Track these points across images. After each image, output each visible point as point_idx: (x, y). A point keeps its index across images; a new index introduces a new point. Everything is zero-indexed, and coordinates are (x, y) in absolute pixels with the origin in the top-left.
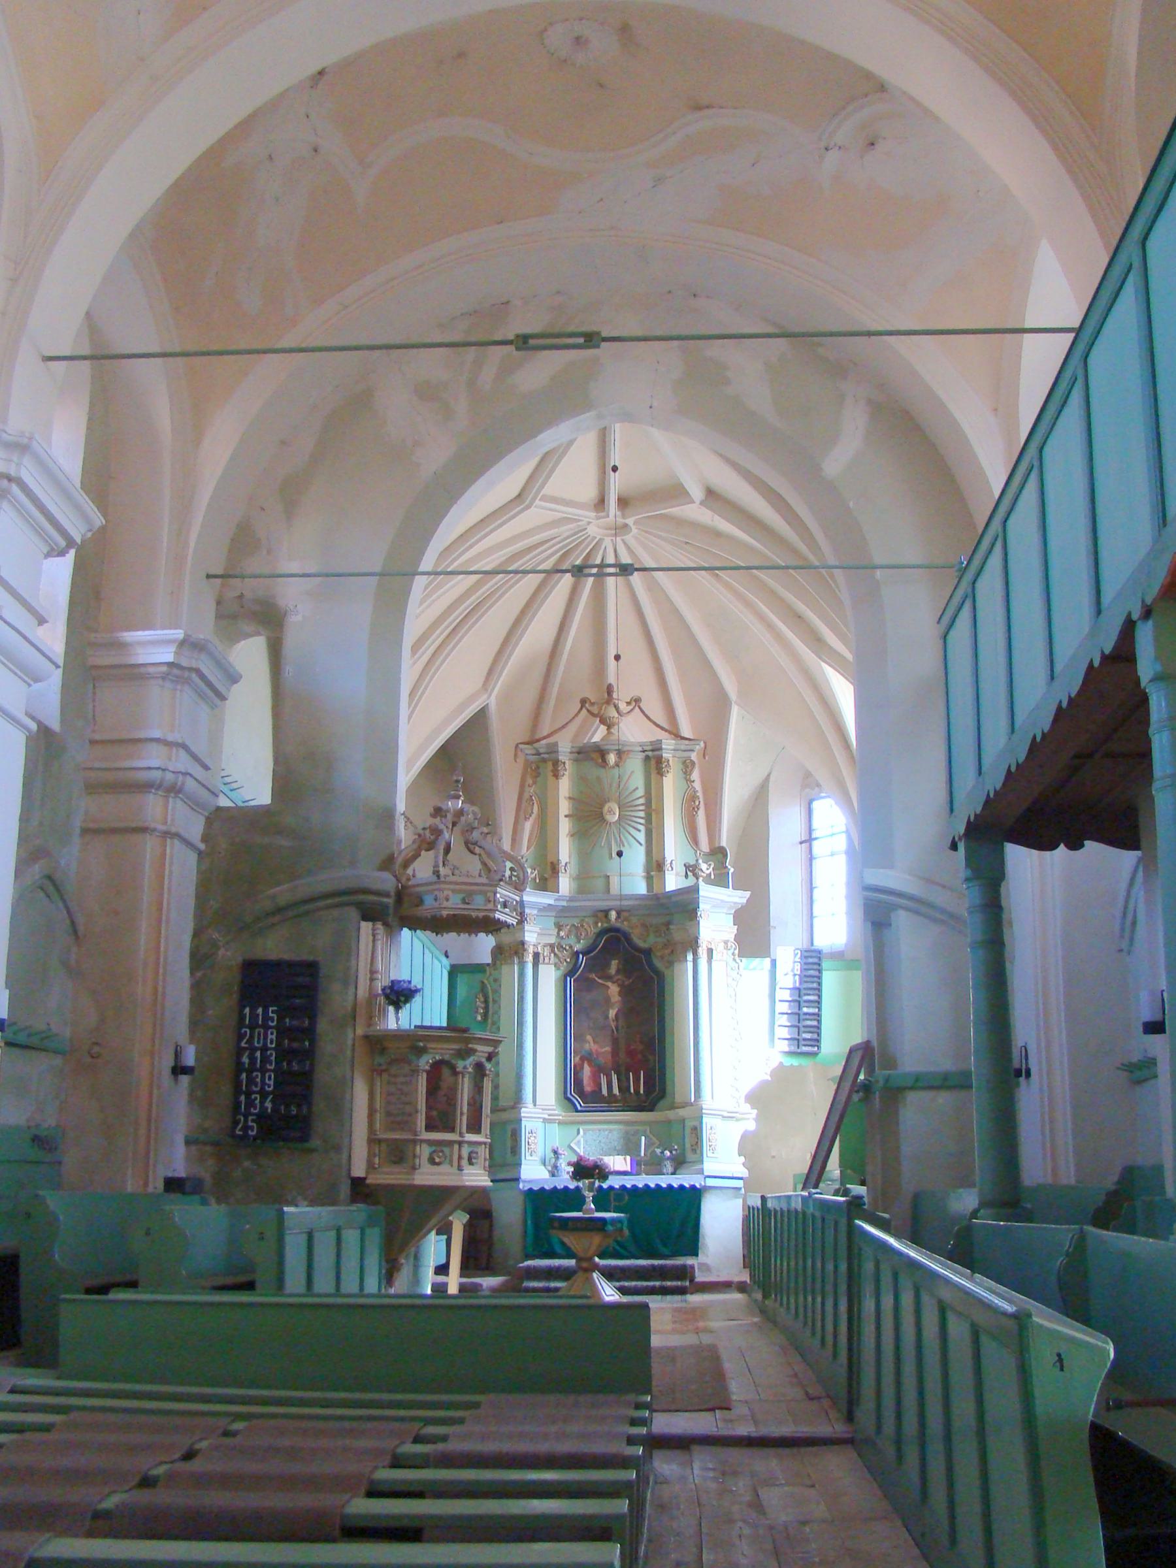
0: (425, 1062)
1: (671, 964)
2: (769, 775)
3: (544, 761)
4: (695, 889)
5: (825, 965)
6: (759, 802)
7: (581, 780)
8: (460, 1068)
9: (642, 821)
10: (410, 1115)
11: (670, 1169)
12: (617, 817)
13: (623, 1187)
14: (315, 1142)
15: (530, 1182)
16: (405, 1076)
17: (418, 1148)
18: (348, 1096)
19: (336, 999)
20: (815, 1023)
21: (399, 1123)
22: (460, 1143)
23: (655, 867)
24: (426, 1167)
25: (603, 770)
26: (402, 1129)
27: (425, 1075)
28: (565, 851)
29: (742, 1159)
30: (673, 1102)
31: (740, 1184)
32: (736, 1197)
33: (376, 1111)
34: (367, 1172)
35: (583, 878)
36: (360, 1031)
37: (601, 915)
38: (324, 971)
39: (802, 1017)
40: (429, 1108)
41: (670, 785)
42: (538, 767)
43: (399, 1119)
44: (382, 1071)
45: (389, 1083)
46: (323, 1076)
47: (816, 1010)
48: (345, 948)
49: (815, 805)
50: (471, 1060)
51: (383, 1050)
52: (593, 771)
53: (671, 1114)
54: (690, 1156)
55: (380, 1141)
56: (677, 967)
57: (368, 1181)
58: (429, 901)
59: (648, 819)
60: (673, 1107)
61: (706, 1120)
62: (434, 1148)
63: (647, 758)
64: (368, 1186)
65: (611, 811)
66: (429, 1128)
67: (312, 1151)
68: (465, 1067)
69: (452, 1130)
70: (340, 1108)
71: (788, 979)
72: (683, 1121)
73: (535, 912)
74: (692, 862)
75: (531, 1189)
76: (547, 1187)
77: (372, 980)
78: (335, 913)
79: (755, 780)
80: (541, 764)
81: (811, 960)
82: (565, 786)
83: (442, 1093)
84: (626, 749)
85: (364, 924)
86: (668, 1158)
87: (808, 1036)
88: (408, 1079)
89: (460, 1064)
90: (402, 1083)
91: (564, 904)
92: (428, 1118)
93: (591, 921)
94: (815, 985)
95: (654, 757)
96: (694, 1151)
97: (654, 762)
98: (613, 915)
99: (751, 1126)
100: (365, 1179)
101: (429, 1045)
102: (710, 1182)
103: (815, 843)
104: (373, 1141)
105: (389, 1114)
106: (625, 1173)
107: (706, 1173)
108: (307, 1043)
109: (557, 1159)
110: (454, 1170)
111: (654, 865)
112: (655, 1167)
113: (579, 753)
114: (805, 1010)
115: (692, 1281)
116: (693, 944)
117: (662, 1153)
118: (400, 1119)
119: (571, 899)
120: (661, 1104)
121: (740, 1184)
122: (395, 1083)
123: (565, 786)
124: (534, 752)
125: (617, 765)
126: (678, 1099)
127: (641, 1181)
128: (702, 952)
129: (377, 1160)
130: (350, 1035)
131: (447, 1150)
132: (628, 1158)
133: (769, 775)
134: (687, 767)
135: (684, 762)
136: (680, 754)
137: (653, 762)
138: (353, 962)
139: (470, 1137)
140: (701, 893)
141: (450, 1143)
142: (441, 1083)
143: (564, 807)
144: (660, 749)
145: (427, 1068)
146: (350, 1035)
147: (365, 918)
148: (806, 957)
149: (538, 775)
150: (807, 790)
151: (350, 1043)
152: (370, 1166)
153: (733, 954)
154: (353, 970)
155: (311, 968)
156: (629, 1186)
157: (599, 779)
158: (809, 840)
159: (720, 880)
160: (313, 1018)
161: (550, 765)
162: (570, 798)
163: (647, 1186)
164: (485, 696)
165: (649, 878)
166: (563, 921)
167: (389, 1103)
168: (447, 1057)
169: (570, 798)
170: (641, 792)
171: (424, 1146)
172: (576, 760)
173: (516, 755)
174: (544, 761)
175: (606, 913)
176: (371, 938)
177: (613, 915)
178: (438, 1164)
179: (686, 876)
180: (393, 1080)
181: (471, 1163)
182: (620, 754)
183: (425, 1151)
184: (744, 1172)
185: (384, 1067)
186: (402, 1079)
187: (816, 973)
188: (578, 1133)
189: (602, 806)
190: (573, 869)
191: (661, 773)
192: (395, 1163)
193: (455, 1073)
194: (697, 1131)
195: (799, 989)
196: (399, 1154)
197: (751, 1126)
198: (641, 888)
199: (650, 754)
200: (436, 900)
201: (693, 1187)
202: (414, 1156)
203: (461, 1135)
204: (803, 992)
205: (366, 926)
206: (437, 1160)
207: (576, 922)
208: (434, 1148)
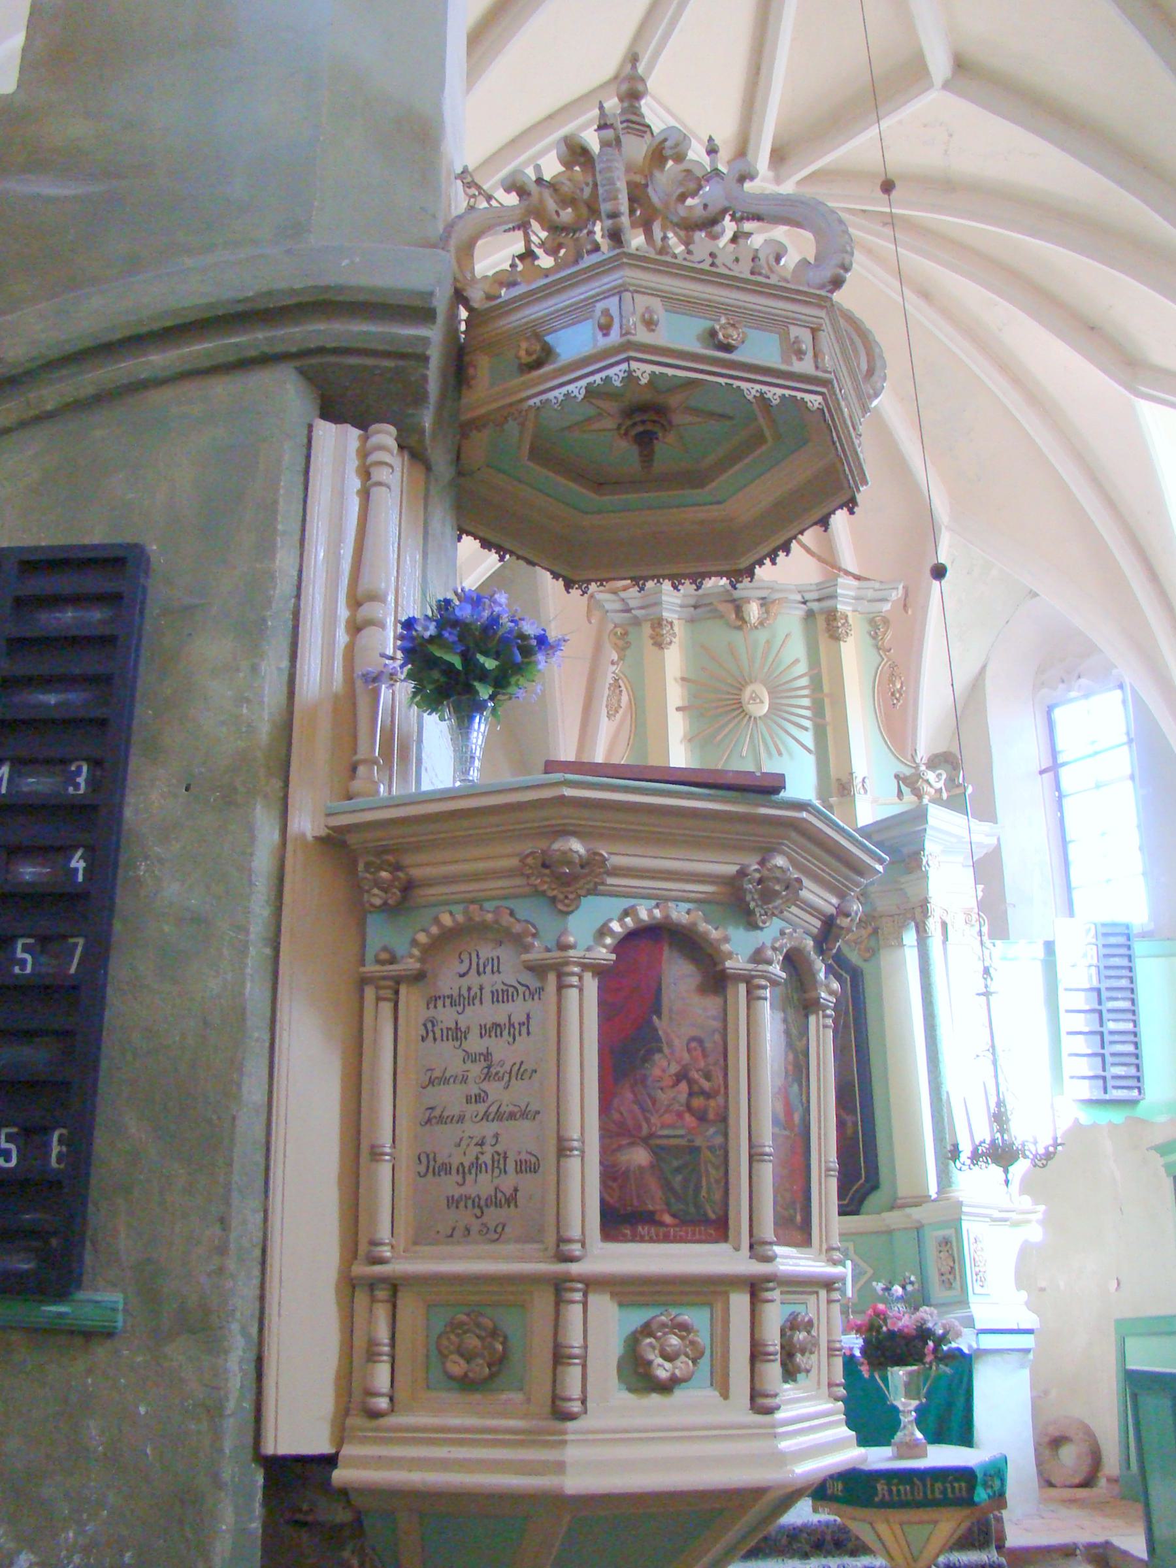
0: (592, 928)
1: (872, 953)
2: (984, 668)
3: (637, 622)
4: (919, 816)
5: (1139, 947)
6: (969, 708)
7: (699, 651)
8: (737, 962)
9: (808, 713)
10: (529, 1166)
14: (103, 1297)
16: (502, 996)
17: (574, 1313)
18: (253, 1090)
19: (208, 694)
20: (1130, 1048)
21: (479, 1205)
22: (559, 1286)
24: (609, 1403)
25: (737, 636)
26: (496, 1234)
27: (591, 985)
29: (1023, 1295)
30: (895, 1199)
31: (1027, 1341)
32: (1022, 1366)
33: (376, 1155)
34: (341, 1435)
36: (306, 823)
38: (163, 590)
39: (1107, 1038)
40: (615, 1132)
41: (854, 658)
42: (626, 634)
43: (483, 1186)
44: (398, 980)
45: (429, 1029)
46: (141, 1006)
47: (1129, 1026)
48: (250, 508)
49: (1057, 714)
50: (773, 933)
51: (404, 898)
52: (718, 635)
53: (893, 1219)
55: (395, 1286)
56: (886, 958)
57: (340, 1475)
58: (574, 342)
59: (818, 709)
60: (894, 1205)
61: (970, 1228)
62: (637, 1317)
63: (810, 615)
64: (344, 1493)
65: (755, 698)
66: (621, 1219)
67: (89, 1335)
68: (758, 957)
69: (717, 1228)
70: (215, 1140)
71: (1079, 970)
72: (919, 1228)
74: (907, 771)
77: (356, 628)
78: (221, 388)
79: (963, 678)
81: (1112, 940)
82: (674, 660)
83: (662, 1067)
84: (777, 596)
85: (326, 431)
86: (900, 1299)
87: (1120, 1071)
88: (517, 1009)
89: (738, 946)
90: (492, 1030)
92: (611, 1175)
94: (1124, 983)
95: (822, 611)
96: (949, 1285)
99: (1035, 1233)
100: (330, 1461)
101: (618, 856)
102: (987, 1342)
103: (1063, 772)
104: (365, 1284)
105: (431, 1166)
107: (979, 1326)
108: (78, 863)
110: (738, 1410)
111: (834, 786)
113: (695, 607)
114: (1112, 1026)
115: (1000, 1548)
116: (916, 913)
117: (887, 1289)
118: (482, 1191)
120: (874, 1200)
121: (1027, 1341)
122: (458, 1034)
123: (674, 660)
124: (618, 606)
125: (761, 623)
126: (904, 1190)
128: (933, 925)
129: (381, 1376)
130: (267, 834)
131: (698, 1318)
133: (984, 668)
134: (877, 626)
135: (872, 622)
136: (864, 606)
137: (821, 622)
138: (284, 560)
139: (791, 1260)
140: (931, 820)
141: (709, 1290)
142: (661, 1025)
143: (675, 695)
144: (833, 596)
145: (603, 954)
146: (267, 834)
147: (331, 411)
148: (1105, 935)
149: (628, 644)
150: (1044, 691)
151: (263, 861)
152: (355, 1406)
153: (980, 933)
154: (284, 587)
155: (108, 575)
157: (732, 650)
158: (1053, 768)
159: (955, 801)
160: (111, 774)
161: (647, 629)
162: (683, 679)
167: (433, 1118)
168: (679, 914)
169: (683, 679)
170: (802, 668)
171: (601, 1303)
172: (691, 621)
174: (637, 622)
176: (355, 483)
178: (666, 1387)
179: (900, 794)
180: (446, 1016)
181: (790, 1373)
182: (764, 603)
183: (602, 1329)
184: (1029, 1320)
185: (411, 965)
186: (490, 1013)
187: (1124, 962)
189: (740, 690)
191: (835, 636)
192: (466, 1384)
193: (716, 980)
194: (951, 1247)
195: (1099, 991)
196: (484, 1347)
197: (1035, 1233)
199: (815, 606)
200: (605, 329)
202: (559, 1357)
203: (757, 1249)
204: (1104, 994)
205: (335, 442)
206: (663, 1371)
208: (637, 1317)
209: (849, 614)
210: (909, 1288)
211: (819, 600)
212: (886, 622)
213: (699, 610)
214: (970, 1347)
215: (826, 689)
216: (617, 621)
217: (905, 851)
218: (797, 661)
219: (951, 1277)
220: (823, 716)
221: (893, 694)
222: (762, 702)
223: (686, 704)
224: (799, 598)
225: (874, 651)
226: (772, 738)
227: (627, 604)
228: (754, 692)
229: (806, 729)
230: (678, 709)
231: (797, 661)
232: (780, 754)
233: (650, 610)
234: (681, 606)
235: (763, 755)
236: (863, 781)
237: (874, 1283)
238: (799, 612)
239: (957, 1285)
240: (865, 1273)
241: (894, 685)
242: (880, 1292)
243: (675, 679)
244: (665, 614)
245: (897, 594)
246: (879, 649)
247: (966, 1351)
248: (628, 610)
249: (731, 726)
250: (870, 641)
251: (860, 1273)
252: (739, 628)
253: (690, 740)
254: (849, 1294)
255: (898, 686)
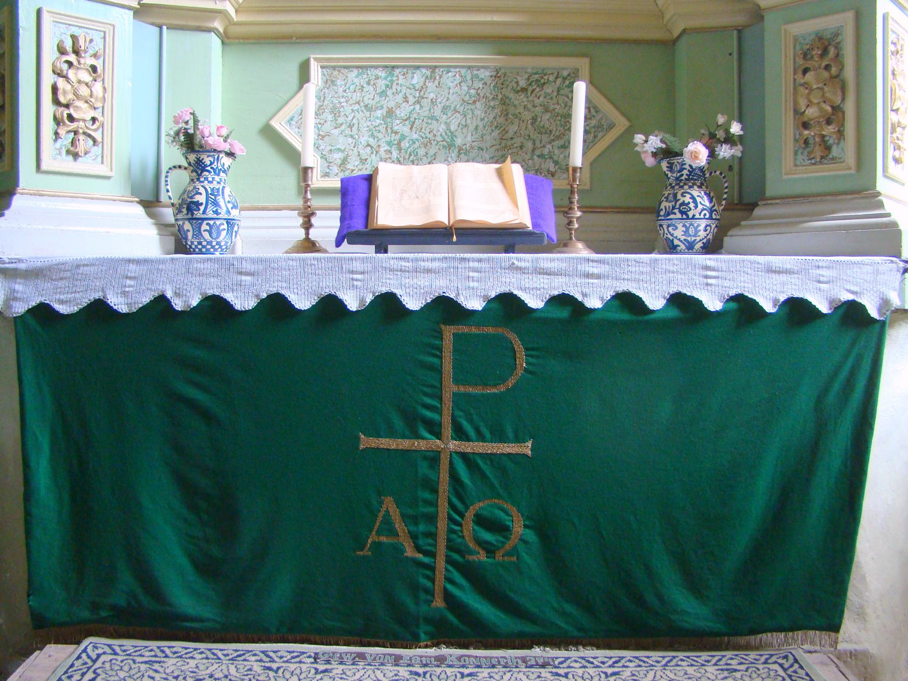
11: (702, 229)
13: (508, 306)
15: (35, 274)
54: (786, 170)
75: (43, 312)
76: (119, 303)
86: (697, 177)
96: (819, 149)
106: (503, 238)
109: (199, 169)
112: (634, 214)
117: (668, 153)
127: (592, 277)
132: (516, 172)
156: (535, 302)
163: (628, 301)
188: (304, 77)
201: (852, 314)
210: (725, 152)
214: (885, 303)
219: (830, 130)
237: (639, 138)
239: (847, 149)
240: (611, 126)
242: (650, 161)
247: (873, 313)
251: (599, 127)
254: (577, 157)
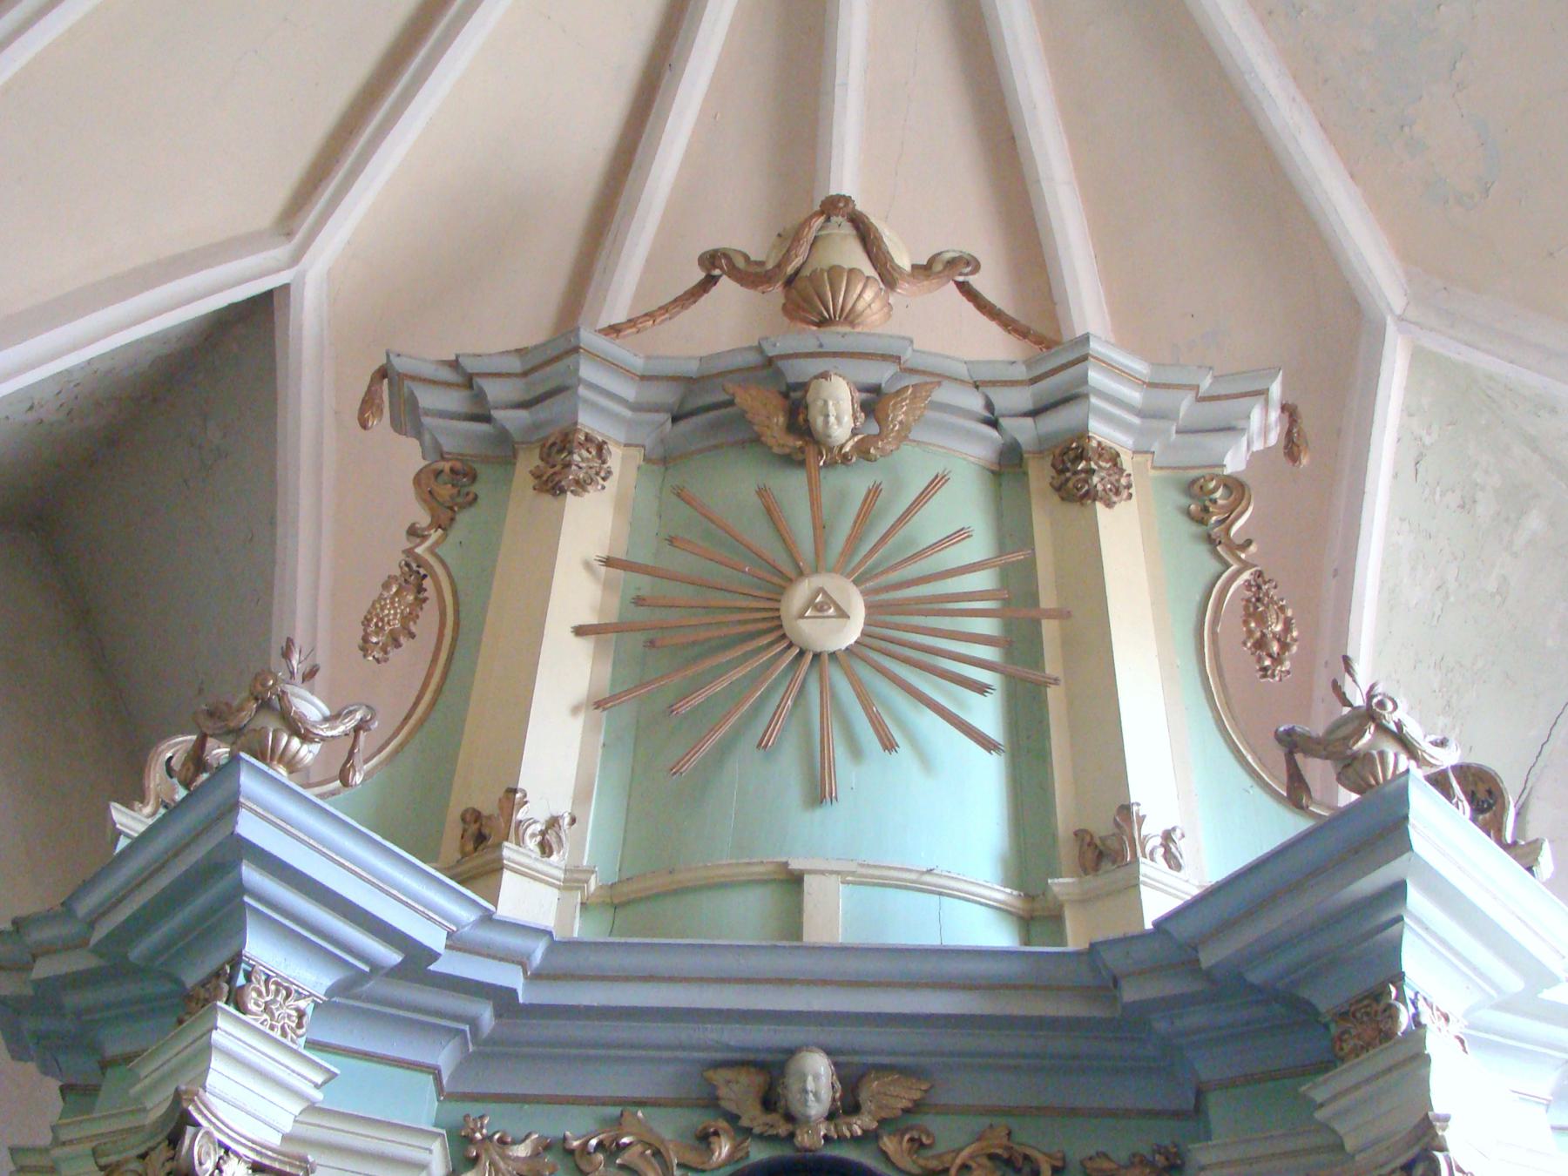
12: (851, 632)
23: (1071, 836)
28: (557, 757)
35: (636, 898)
37: (739, 1091)
41: (1134, 551)
52: (734, 485)
63: (1008, 465)
73: (315, 979)
80: (493, 444)
82: (590, 524)
91: (510, 977)
93: (669, 1127)
95: (1043, 446)
97: (1050, 470)
98: (817, 1077)
111: (1067, 851)
119: (565, 959)
125: (863, 450)
137: (1039, 475)
143: (575, 595)
161: (528, 462)
162: (608, 562)
164: (281, 252)
165: (1036, 915)
166: (493, 1121)
169: (608, 562)
170: (978, 547)
172: (663, 460)
173: (369, 403)
174: (504, 449)
175: (771, 1076)
177: (817, 1077)
182: (873, 402)
189: (781, 583)
190: (594, 847)
198: (997, 935)
199: (1024, 431)
207: (578, 1128)
209: (1126, 461)
211: (1034, 413)
212: (1237, 488)
213: (684, 426)
215: (1047, 600)
216: (448, 445)
217: (1326, 998)
218: (961, 535)
220: (1037, 661)
221: (1261, 644)
222: (842, 614)
223: (612, 618)
224: (975, 403)
225: (1202, 550)
226: (867, 706)
227: (480, 397)
228: (821, 590)
229: (981, 689)
230: (580, 631)
231: (961, 535)
232: (889, 745)
233: (543, 412)
234: (637, 407)
235: (840, 753)
236: (1167, 837)
238: (980, 448)
241: (1262, 620)
243: (587, 566)
244: (588, 422)
245: (1262, 427)
246: (1211, 541)
248: (486, 419)
249: (736, 675)
250: (1188, 528)
252: (792, 461)
253: (599, 704)
255: (1278, 628)
